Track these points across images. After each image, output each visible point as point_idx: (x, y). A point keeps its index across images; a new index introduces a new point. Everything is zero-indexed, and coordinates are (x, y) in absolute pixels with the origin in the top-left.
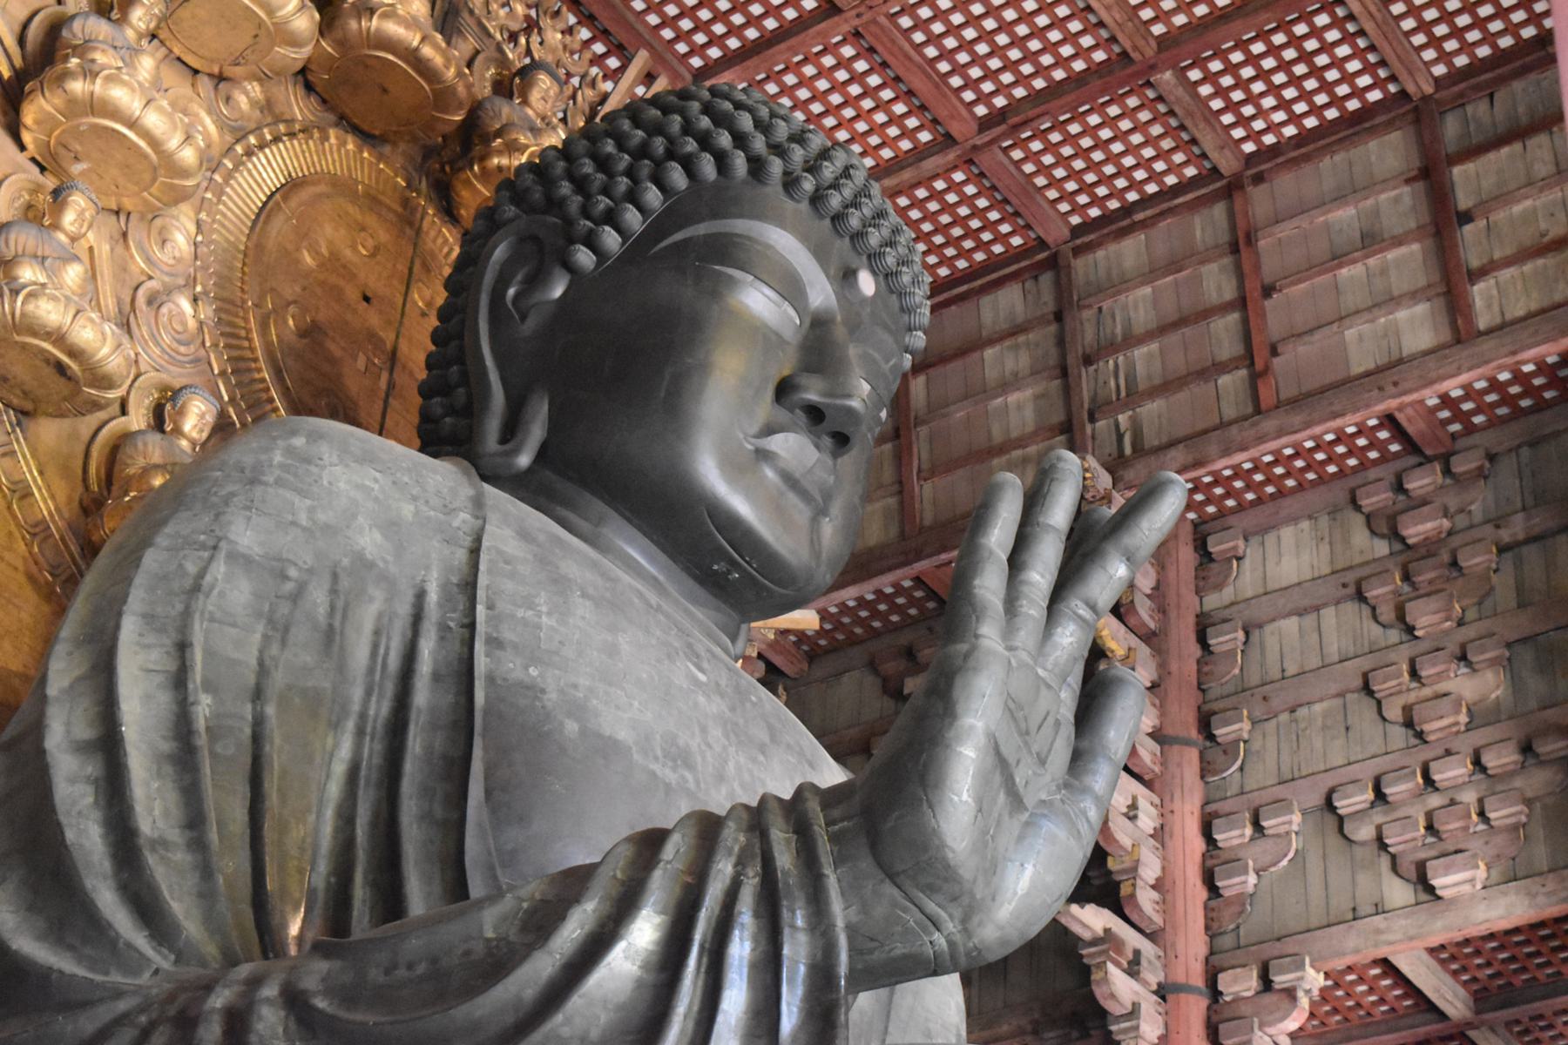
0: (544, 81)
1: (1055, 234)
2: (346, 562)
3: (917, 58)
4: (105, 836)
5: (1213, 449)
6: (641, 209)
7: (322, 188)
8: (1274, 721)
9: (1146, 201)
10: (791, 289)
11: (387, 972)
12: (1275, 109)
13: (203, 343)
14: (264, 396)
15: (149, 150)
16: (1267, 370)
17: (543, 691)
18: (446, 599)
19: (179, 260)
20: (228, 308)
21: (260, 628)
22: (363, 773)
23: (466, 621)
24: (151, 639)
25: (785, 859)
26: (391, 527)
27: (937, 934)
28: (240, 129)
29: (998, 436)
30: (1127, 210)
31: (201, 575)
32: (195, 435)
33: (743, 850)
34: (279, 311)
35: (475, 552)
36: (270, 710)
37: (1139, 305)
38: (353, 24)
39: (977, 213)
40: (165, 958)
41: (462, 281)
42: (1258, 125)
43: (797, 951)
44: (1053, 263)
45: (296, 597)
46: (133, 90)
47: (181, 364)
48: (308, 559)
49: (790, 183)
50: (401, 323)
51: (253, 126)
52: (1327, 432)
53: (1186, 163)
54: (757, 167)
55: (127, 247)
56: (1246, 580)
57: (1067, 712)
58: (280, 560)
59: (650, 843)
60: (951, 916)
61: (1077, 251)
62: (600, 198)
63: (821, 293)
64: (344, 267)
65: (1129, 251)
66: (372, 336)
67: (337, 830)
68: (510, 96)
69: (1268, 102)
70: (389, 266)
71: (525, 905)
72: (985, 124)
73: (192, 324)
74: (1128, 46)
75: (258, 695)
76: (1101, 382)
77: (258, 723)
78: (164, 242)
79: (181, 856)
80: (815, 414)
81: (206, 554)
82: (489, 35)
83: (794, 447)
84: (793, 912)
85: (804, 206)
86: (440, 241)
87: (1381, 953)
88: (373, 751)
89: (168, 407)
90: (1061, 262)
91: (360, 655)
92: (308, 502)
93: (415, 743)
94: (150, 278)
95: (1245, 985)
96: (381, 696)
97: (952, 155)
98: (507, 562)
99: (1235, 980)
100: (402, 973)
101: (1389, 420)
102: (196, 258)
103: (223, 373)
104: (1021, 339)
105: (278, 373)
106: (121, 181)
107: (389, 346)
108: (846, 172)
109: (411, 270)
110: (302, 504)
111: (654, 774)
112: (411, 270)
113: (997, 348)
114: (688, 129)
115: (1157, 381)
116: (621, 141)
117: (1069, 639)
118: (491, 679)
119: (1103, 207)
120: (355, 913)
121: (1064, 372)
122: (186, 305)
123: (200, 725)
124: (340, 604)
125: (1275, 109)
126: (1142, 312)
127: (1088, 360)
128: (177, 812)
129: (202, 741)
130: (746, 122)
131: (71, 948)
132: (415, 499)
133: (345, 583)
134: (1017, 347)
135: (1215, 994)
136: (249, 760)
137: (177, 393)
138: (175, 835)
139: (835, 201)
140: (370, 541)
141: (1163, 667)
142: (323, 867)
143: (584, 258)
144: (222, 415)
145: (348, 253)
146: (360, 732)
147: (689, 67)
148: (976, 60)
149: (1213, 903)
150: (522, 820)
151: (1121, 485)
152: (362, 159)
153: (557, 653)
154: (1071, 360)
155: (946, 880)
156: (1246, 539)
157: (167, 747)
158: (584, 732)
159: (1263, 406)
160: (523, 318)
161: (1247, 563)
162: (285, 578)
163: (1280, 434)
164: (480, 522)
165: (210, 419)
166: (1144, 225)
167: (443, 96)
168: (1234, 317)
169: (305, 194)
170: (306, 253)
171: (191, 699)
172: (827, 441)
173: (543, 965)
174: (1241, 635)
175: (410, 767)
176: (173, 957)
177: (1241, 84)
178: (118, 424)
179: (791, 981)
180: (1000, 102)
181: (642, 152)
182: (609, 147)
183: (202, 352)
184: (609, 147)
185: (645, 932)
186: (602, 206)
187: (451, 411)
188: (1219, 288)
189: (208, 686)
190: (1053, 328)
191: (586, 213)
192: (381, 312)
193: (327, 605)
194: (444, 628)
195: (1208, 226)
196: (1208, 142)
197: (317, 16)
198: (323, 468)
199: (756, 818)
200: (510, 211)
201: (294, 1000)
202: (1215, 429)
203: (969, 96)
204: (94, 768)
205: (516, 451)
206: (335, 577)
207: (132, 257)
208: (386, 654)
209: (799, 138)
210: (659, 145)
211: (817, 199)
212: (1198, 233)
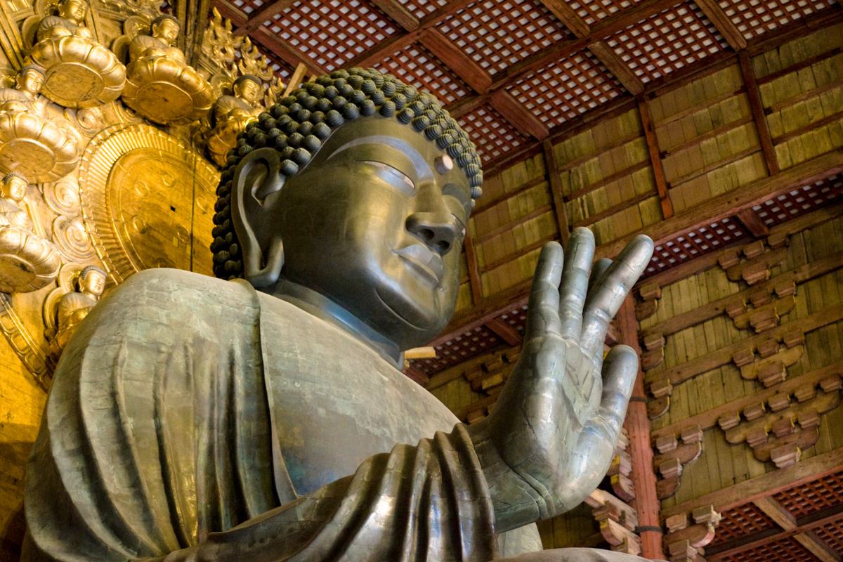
2: (190, 340)
3: (455, 48)
4: (91, 497)
6: (320, 136)
7: (141, 156)
9: (589, 111)
10: (409, 172)
13: (92, 244)
16: (666, 196)
21: (152, 379)
24: (97, 393)
30: (580, 117)
31: (116, 359)
32: (96, 291)
36: (164, 421)
37: (592, 169)
40: (132, 554)
41: (225, 191)
44: (541, 149)
48: (170, 340)
52: (701, 228)
59: (380, 462)
61: (554, 142)
63: (425, 172)
64: (159, 194)
65: (584, 140)
66: (179, 228)
70: (182, 190)
71: (318, 502)
72: (495, 78)
73: (85, 236)
75: (156, 414)
77: (159, 429)
79: (131, 502)
85: (409, 126)
90: (546, 149)
92: (166, 311)
100: (257, 545)
103: (104, 258)
105: (133, 253)
109: (194, 191)
110: (163, 313)
112: (194, 191)
114: (341, 92)
115: (606, 207)
116: (304, 104)
119: (566, 117)
123: (130, 433)
124: (191, 362)
126: (593, 171)
128: (126, 481)
129: (132, 441)
130: (372, 84)
132: (220, 303)
136: (156, 449)
138: (127, 492)
143: (292, 166)
144: (108, 279)
145: (159, 187)
152: (159, 137)
157: (115, 447)
159: (666, 216)
162: (160, 352)
163: (676, 229)
165: (103, 282)
170: (137, 189)
171: (123, 421)
173: (332, 532)
176: (136, 553)
178: (56, 293)
180: (503, 66)
181: (317, 107)
183: (92, 249)
184: (297, 106)
185: (384, 507)
189: (132, 414)
192: (181, 214)
198: (170, 292)
199: (435, 445)
200: (248, 147)
204: (79, 463)
206: (186, 348)
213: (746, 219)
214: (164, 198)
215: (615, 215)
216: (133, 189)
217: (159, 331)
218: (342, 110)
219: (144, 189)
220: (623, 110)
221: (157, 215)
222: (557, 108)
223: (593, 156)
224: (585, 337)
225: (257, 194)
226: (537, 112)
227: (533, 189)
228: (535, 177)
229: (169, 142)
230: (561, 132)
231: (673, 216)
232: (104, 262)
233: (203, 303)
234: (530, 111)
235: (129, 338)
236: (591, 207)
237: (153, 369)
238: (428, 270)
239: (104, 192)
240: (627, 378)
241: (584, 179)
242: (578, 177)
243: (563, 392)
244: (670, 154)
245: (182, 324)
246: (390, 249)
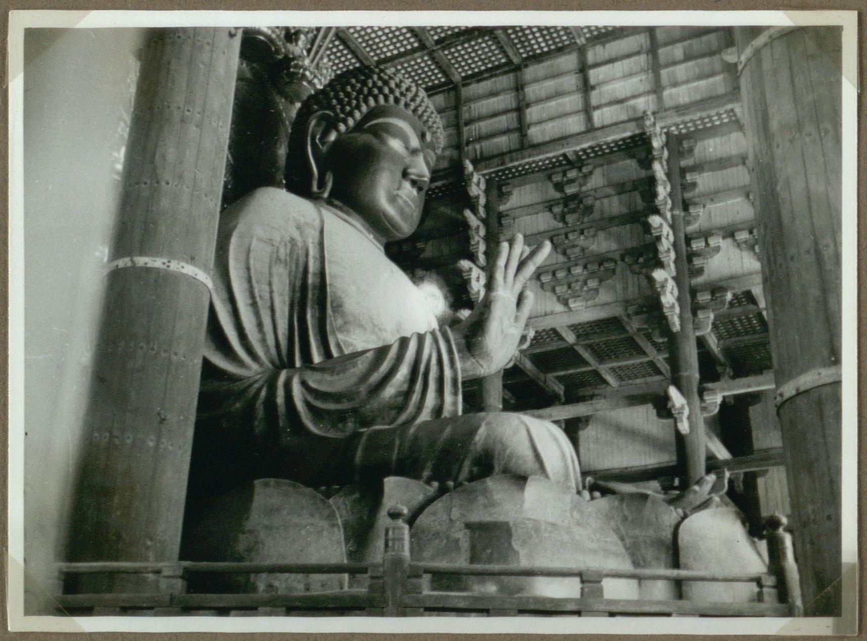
6: (360, 111)
9: (487, 70)
30: (481, 73)
35: (322, 232)
45: (277, 252)
49: (407, 105)
54: (397, 100)
61: (464, 85)
75: (270, 284)
87: (554, 326)
97: (425, 52)
101: (564, 155)
108: (422, 101)
116: (353, 87)
118: (330, 275)
127: (466, 124)
168: (514, 115)
181: (360, 92)
182: (349, 89)
184: (349, 89)
190: (454, 112)
191: (343, 110)
194: (315, 258)
196: (510, 53)
201: (304, 384)
205: (324, 192)
210: (366, 90)
211: (415, 111)
213: (572, 157)
218: (376, 98)
225: (320, 139)
226: (457, 66)
230: (467, 80)
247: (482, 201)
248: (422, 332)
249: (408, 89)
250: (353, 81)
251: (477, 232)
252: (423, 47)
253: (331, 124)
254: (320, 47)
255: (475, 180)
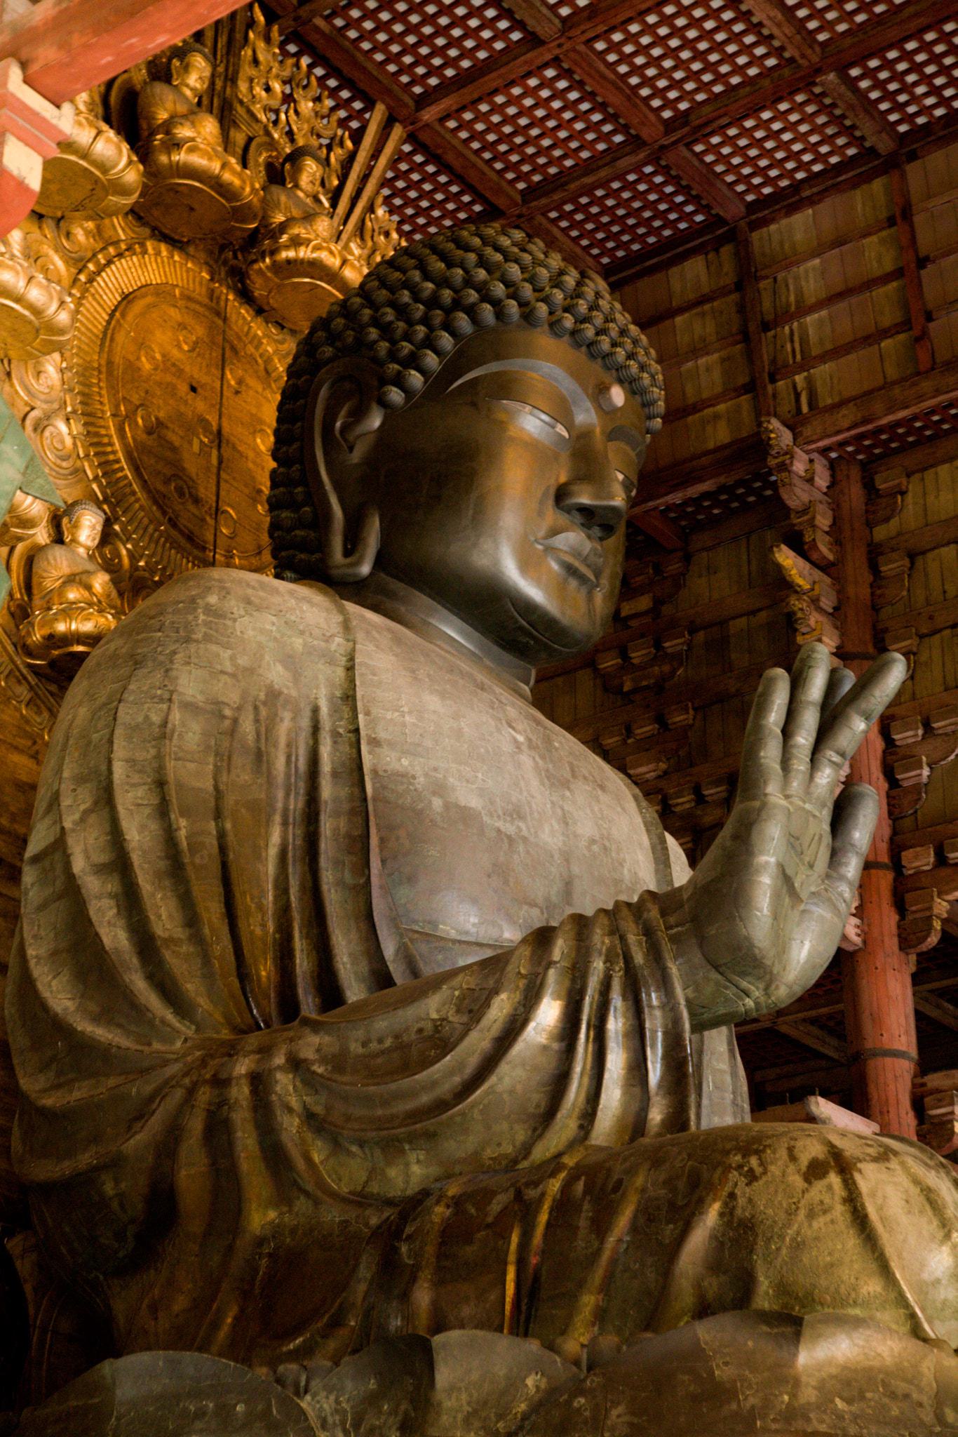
0: (311, 168)
1: (732, 211)
2: (262, 696)
3: (612, 76)
4: (130, 939)
5: (878, 407)
6: (437, 352)
7: (149, 299)
8: (938, 636)
9: (813, 177)
11: (364, 1045)
12: (926, 95)
14: (128, 490)
15: (32, 318)
17: (414, 777)
18: (334, 710)
19: (51, 388)
20: (90, 419)
21: (211, 759)
22: (290, 854)
23: (351, 727)
24: (136, 778)
25: (639, 958)
26: (289, 661)
27: (747, 1000)
28: (81, 260)
29: (691, 400)
30: (796, 186)
31: (165, 723)
32: (89, 543)
33: (609, 951)
34: (131, 417)
35: (350, 668)
36: (228, 826)
37: (810, 278)
38: (163, 159)
39: (664, 198)
40: (189, 1028)
42: (911, 109)
43: (655, 1023)
46: (17, 273)
47: (65, 477)
48: (233, 697)
50: (221, 404)
51: (89, 254)
53: (847, 145)
55: (12, 385)
56: (910, 513)
57: (826, 827)
58: (218, 703)
60: (758, 988)
62: (404, 344)
63: (585, 415)
64: (174, 365)
65: (798, 227)
66: (202, 421)
67: (276, 897)
68: (282, 183)
69: (920, 90)
70: (207, 356)
71: (457, 993)
72: (669, 125)
73: (69, 441)
74: (797, 55)
75: (218, 815)
76: (779, 347)
77: (221, 835)
78: (39, 373)
79: (184, 949)
80: (588, 515)
81: (165, 706)
82: (257, 120)
83: (573, 539)
84: (649, 995)
86: (241, 322)
88: (296, 835)
89: (65, 521)
91: (280, 764)
92: (229, 652)
93: (327, 826)
94: (33, 409)
95: (925, 861)
96: (297, 794)
97: (642, 156)
98: (374, 675)
99: (916, 857)
102: (64, 383)
103: (96, 478)
104: (707, 307)
105: (137, 470)
106: (9, 340)
107: (215, 428)
109: (223, 355)
111: (499, 831)
112: (223, 355)
113: (687, 315)
114: (469, 282)
115: (829, 346)
117: (827, 779)
119: (775, 185)
120: (298, 961)
121: (745, 336)
122: (63, 428)
124: (263, 730)
125: (926, 95)
126: (812, 281)
127: (766, 327)
130: (514, 270)
131: (120, 1026)
132: (302, 633)
133: (264, 712)
134: (703, 314)
135: (896, 864)
137: (70, 508)
138: (180, 933)
139: (590, 332)
140: (276, 674)
141: (841, 593)
142: (271, 927)
143: (396, 395)
145: (175, 353)
146: (285, 823)
147: (413, 95)
148: (663, 73)
149: (894, 793)
150: (411, 880)
151: (800, 440)
153: (419, 745)
154: (752, 327)
155: (755, 967)
156: (908, 476)
157: (163, 865)
158: (447, 806)
160: (351, 449)
161: (909, 498)
162: (224, 717)
164: (351, 644)
165: (99, 528)
166: (811, 201)
167: (242, 213)
169: (138, 306)
170: (143, 359)
171: (175, 826)
172: (597, 531)
174: (907, 562)
175: (326, 846)
176: (193, 1027)
177: (896, 77)
179: (653, 1046)
180: (683, 106)
181: (433, 302)
182: (406, 296)
184: (406, 296)
185: (549, 1012)
186: (406, 351)
187: (300, 524)
188: (879, 261)
189: (182, 815)
191: (393, 356)
192: (205, 398)
193: (253, 733)
194: (335, 735)
195: (867, 201)
196: (866, 128)
197: (141, 167)
198: (235, 620)
199: (612, 915)
200: (328, 351)
202: (880, 389)
203: (656, 103)
204: (113, 885)
205: (359, 563)
206: (256, 708)
207: (17, 392)
208: (297, 760)
209: (556, 282)
210: (447, 294)
212: (859, 207)
214: (181, 371)
215: (843, 360)
216: (138, 359)
217: (221, 685)
218: (471, 311)
219: (154, 358)
220: (866, 178)
221: (171, 402)
222: (762, 172)
223: (813, 255)
224: (812, 789)
226: (730, 178)
227: (715, 304)
228: (722, 284)
229: (188, 270)
231: (933, 369)
232: (95, 486)
233: (278, 636)
234: (719, 175)
235: (181, 694)
236: (804, 341)
237: (213, 743)
238: (583, 569)
239: (96, 365)
240: (866, 827)
241: (796, 296)
242: (788, 290)
243: (784, 870)
244: (934, 262)
245: (250, 671)
246: (533, 539)
247: (824, 521)
248: (589, 912)
249: (556, 282)
250: (416, 275)
251: (815, 601)
252: (635, 142)
253: (363, 388)
254: (365, 178)
255: (799, 467)
